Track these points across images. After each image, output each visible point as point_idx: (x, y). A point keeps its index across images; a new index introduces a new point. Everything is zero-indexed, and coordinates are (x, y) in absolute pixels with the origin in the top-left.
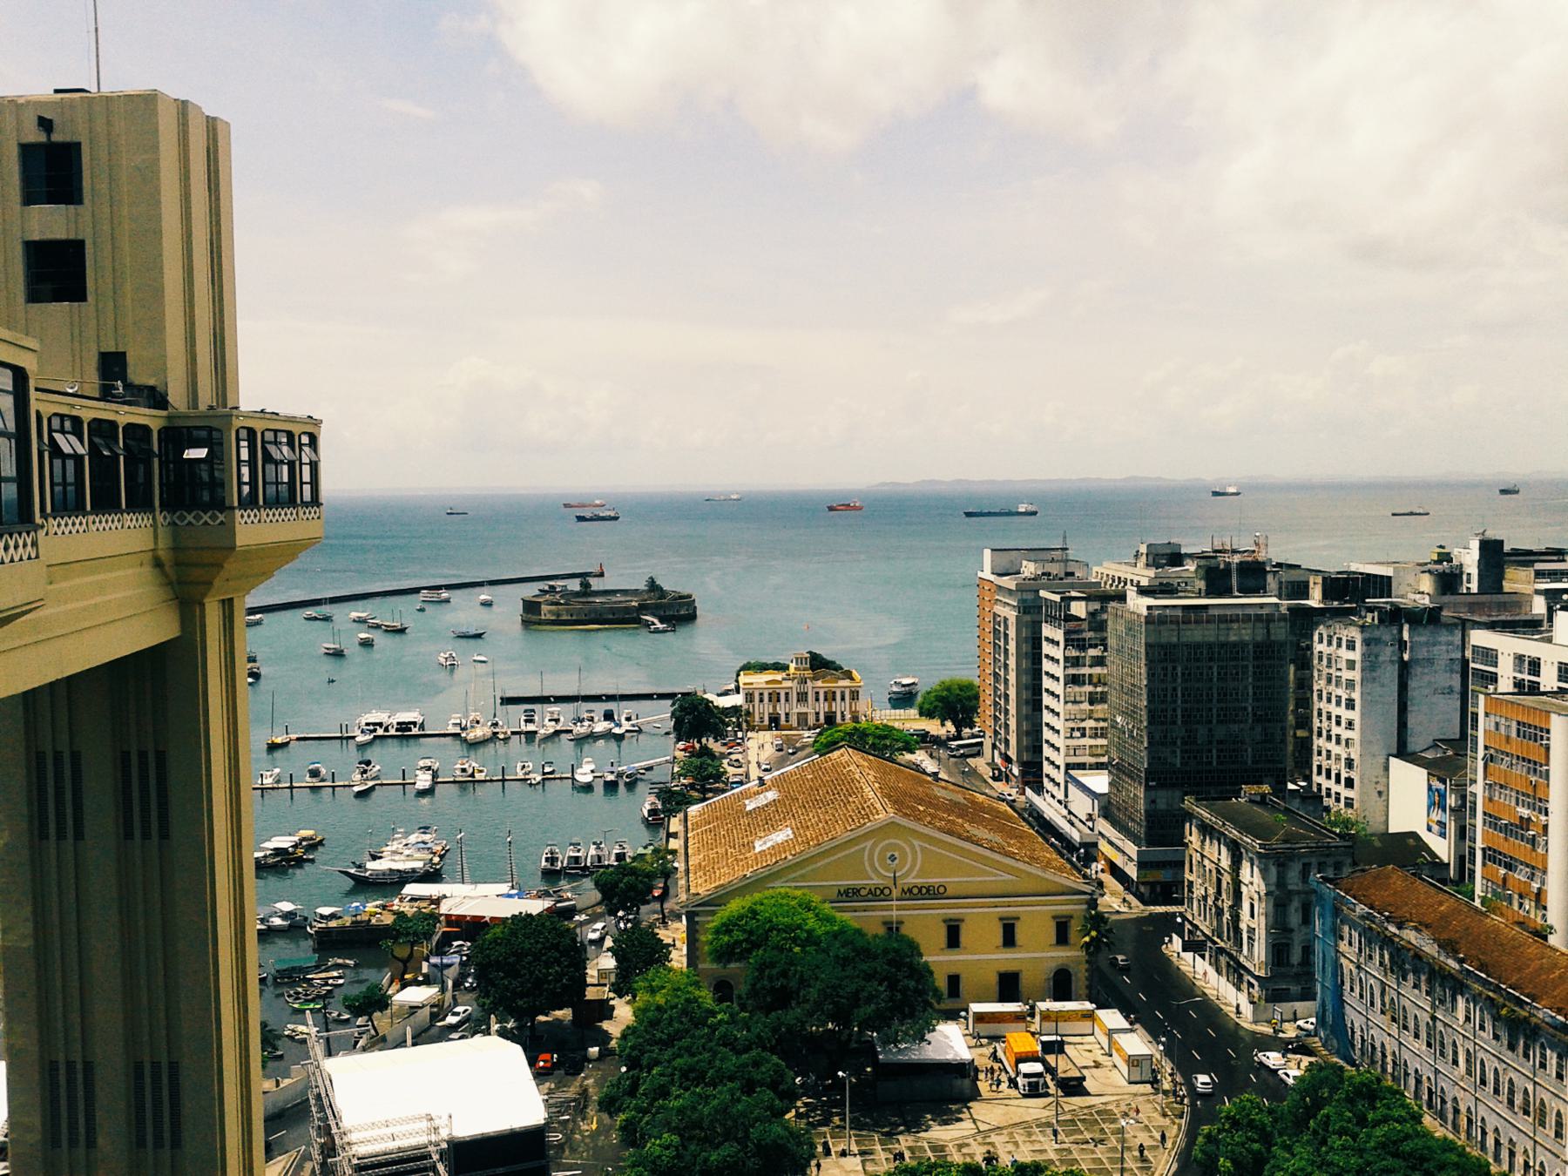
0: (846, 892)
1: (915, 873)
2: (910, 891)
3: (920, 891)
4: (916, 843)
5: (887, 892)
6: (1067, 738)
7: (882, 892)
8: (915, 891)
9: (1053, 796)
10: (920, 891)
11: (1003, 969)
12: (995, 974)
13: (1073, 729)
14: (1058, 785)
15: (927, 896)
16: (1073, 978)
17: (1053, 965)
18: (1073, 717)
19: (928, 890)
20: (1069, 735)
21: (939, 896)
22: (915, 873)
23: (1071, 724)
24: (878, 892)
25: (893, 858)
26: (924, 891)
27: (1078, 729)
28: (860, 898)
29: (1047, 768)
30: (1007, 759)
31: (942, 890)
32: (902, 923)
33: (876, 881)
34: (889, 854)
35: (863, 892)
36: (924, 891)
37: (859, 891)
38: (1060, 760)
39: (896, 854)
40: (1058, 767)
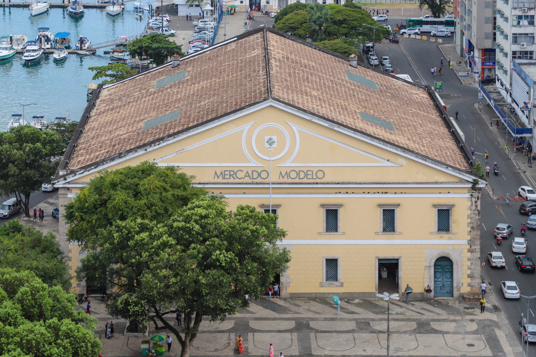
0: (223, 175)
1: (293, 157)
2: (288, 175)
3: (298, 175)
4: (294, 128)
5: (264, 175)
6: (513, 26)
7: (259, 175)
8: (293, 175)
9: (502, 85)
10: (298, 175)
11: (383, 256)
12: (374, 259)
13: (520, 17)
14: (506, 72)
15: (305, 180)
16: (455, 267)
17: (436, 254)
18: (521, 5)
19: (306, 175)
20: (515, 23)
21: (318, 181)
22: (293, 157)
23: (520, 13)
24: (255, 175)
25: (270, 142)
26: (302, 175)
27: (527, 17)
28: (237, 181)
29: (499, 56)
30: (471, 47)
31: (320, 175)
32: (279, 206)
33: (254, 164)
34: (267, 138)
35: (240, 175)
36: (302, 175)
37: (235, 173)
38: (508, 46)
39: (275, 138)
40: (506, 55)
